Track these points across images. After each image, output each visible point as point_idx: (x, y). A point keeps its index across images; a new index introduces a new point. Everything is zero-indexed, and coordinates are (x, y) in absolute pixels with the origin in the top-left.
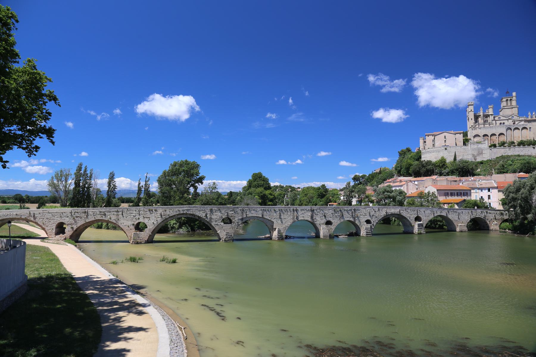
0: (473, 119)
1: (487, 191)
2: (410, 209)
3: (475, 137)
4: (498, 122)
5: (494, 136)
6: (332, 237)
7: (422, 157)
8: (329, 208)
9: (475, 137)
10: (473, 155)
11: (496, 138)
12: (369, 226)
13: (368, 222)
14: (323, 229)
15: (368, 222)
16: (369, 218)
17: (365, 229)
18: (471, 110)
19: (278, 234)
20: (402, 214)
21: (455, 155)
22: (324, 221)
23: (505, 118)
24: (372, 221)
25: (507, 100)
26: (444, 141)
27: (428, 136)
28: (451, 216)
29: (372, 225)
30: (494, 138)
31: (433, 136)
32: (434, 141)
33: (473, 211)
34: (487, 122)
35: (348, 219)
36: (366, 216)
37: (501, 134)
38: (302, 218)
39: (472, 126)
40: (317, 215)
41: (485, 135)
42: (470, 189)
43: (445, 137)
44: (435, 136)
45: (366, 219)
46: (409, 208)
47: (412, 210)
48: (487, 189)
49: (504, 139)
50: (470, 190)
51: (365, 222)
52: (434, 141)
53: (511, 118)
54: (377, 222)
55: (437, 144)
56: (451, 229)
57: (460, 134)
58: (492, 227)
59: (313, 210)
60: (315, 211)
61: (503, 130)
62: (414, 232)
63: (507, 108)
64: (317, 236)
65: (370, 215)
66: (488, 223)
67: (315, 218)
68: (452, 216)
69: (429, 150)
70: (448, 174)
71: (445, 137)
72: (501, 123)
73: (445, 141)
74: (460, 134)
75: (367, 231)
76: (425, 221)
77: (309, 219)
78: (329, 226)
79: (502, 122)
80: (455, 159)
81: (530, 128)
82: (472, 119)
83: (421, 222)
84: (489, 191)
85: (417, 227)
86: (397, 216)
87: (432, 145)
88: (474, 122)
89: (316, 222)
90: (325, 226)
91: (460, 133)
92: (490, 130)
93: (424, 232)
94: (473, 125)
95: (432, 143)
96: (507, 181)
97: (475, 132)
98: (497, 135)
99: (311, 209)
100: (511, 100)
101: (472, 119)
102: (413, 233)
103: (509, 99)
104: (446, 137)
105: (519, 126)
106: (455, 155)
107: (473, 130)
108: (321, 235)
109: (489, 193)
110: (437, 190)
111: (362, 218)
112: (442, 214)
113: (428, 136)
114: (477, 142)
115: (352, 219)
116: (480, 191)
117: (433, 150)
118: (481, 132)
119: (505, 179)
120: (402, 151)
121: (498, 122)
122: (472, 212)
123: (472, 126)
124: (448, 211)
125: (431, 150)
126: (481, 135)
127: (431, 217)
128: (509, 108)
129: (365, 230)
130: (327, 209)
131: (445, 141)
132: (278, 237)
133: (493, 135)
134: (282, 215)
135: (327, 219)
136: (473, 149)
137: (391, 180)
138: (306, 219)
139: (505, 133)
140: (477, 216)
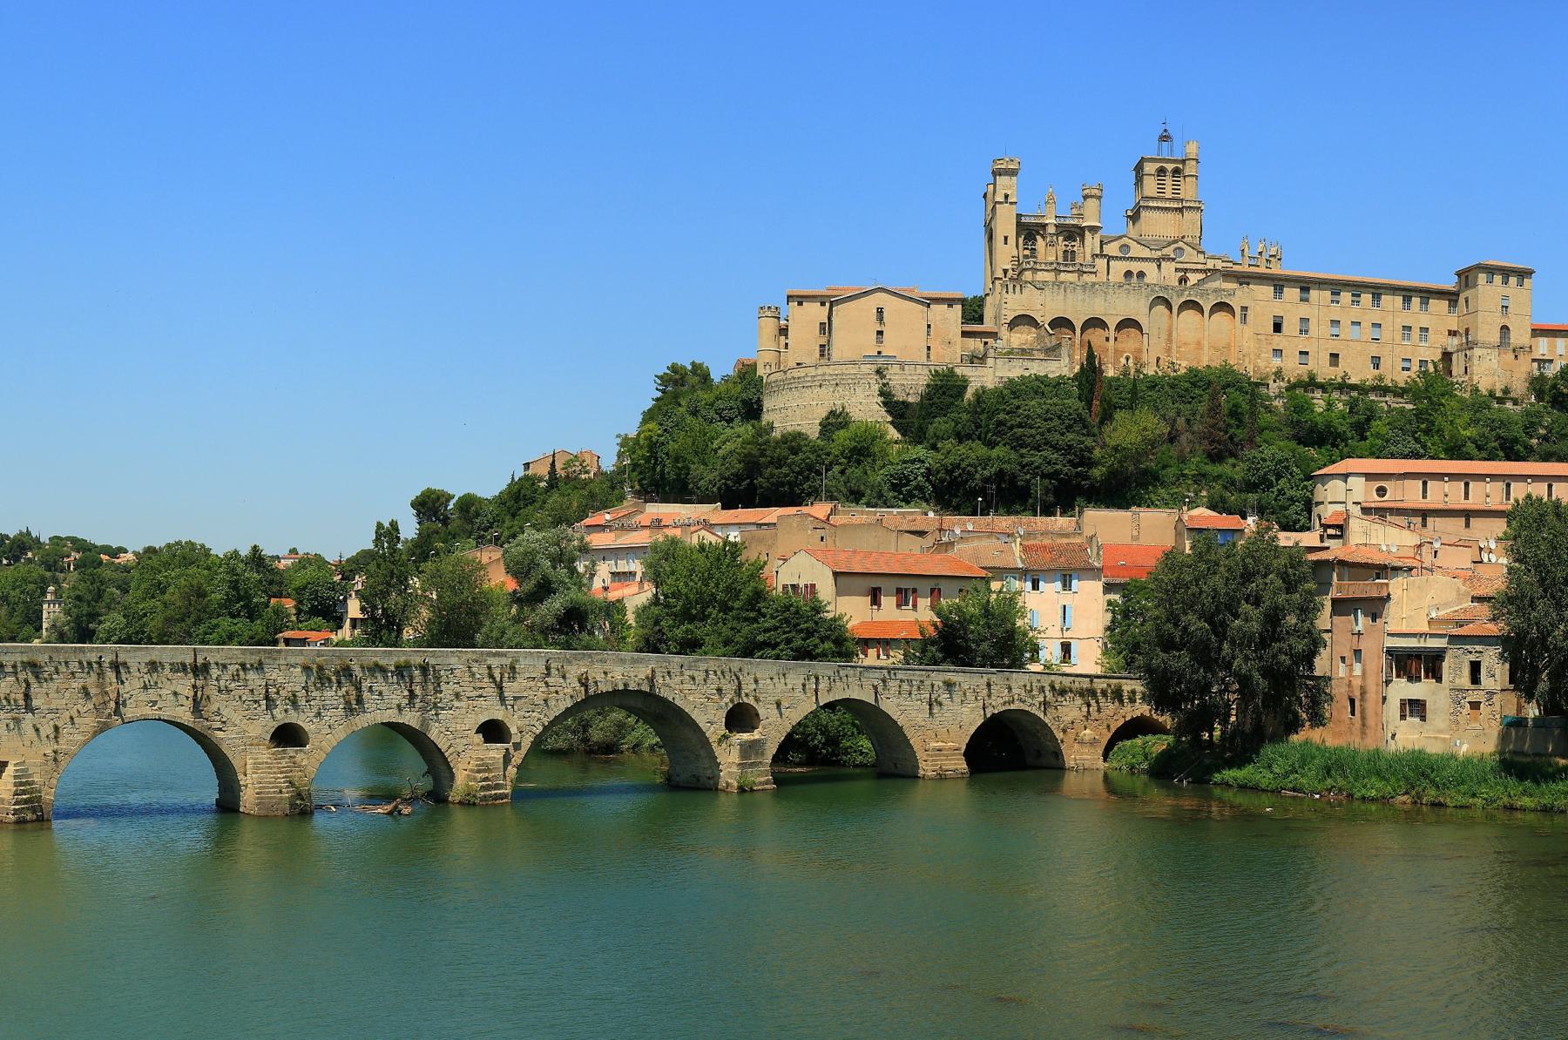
0: (1012, 240)
1: (1058, 585)
2: (703, 666)
3: (1016, 322)
4: (1119, 268)
5: (1099, 331)
6: (302, 809)
7: (768, 404)
8: (292, 660)
9: (1016, 322)
11: (1107, 339)
12: (495, 752)
13: (493, 731)
14: (256, 768)
15: (493, 731)
16: (498, 714)
17: (479, 771)
18: (1006, 196)
19: (16, 794)
20: (664, 693)
22: (264, 725)
23: (1146, 253)
24: (513, 730)
27: (800, 304)
28: (899, 705)
29: (512, 751)
30: (1096, 336)
31: (823, 304)
32: (826, 328)
33: (994, 678)
34: (1073, 259)
35: (391, 716)
36: (481, 701)
37: (1128, 324)
38: (148, 711)
39: (1005, 271)
40: (229, 691)
41: (1061, 323)
42: (983, 573)
44: (831, 303)
45: (483, 719)
46: (698, 660)
47: (715, 672)
48: (1059, 575)
49: (1137, 345)
50: (986, 580)
51: (477, 732)
52: (826, 328)
53: (1172, 256)
54: (538, 732)
55: (841, 348)
56: (896, 768)
57: (950, 306)
58: (1074, 755)
59: (206, 667)
60: (215, 672)
61: (1135, 306)
62: (722, 784)
64: (228, 804)
65: (502, 699)
66: (1059, 735)
67: (214, 707)
68: (902, 708)
69: (801, 373)
70: (880, 500)
72: (1128, 274)
73: (880, 333)
74: (950, 306)
75: (486, 779)
76: (772, 730)
77: (185, 715)
78: (291, 751)
79: (1135, 267)
81: (1244, 309)
82: (1006, 238)
83: (756, 735)
84: (1067, 585)
85: (737, 761)
86: (639, 705)
87: (818, 348)
89: (220, 729)
90: (265, 754)
91: (950, 302)
92: (1084, 300)
93: (767, 783)
94: (1008, 267)
95: (818, 339)
96: (1146, 540)
97: (1015, 303)
98: (1112, 327)
99: (195, 659)
101: (1006, 238)
102: (717, 789)
104: (885, 314)
105: (1202, 295)
107: (1007, 292)
108: (248, 799)
109: (1066, 598)
110: (836, 574)
111: (464, 711)
112: (855, 694)
113: (800, 304)
114: (1023, 350)
115: (411, 718)
116: (1029, 584)
117: (820, 371)
118: (1046, 306)
119: (1135, 533)
120: (674, 368)
121: (1119, 268)
122: (989, 685)
123: (1005, 271)
124: (884, 681)
125: (812, 371)
126: (1044, 319)
127: (808, 706)
129: (479, 776)
130: (282, 662)
131: (880, 333)
132: (16, 812)
133: (1095, 323)
134: (35, 688)
135: (279, 716)
137: (608, 517)
138: (165, 714)
139: (1143, 321)
140: (1012, 707)
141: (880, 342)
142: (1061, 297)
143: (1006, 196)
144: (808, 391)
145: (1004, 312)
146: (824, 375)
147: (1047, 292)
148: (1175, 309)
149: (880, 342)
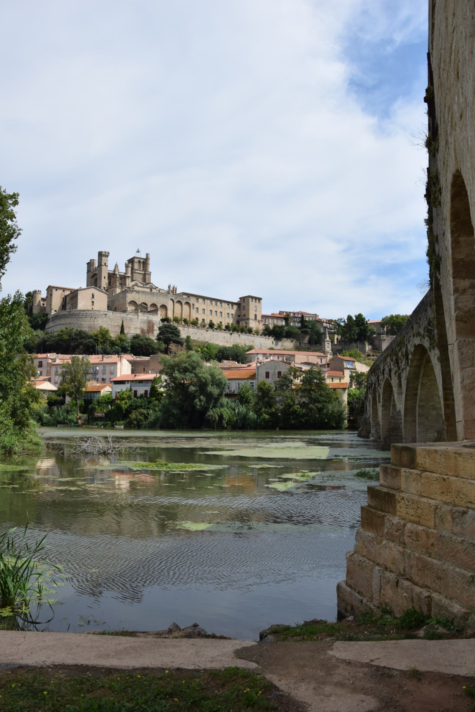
10: (142, 331)
21: (122, 327)
25: (139, 262)
26: (91, 303)
27: (56, 290)
31: (64, 291)
39: (104, 288)
43: (93, 296)
63: (138, 273)
71: (93, 296)
73: (93, 302)
80: (122, 331)
82: (105, 277)
88: (107, 282)
94: (105, 286)
100: (143, 262)
101: (105, 277)
103: (142, 261)
106: (122, 327)
113: (56, 290)
123: (104, 288)
126: (139, 303)
128: (141, 274)
131: (93, 302)
136: (143, 322)
141: (93, 305)
142: (144, 296)
143: (105, 264)
144: (80, 319)
145: (127, 299)
146: (86, 313)
147: (140, 294)
148: (175, 303)
149: (93, 305)
